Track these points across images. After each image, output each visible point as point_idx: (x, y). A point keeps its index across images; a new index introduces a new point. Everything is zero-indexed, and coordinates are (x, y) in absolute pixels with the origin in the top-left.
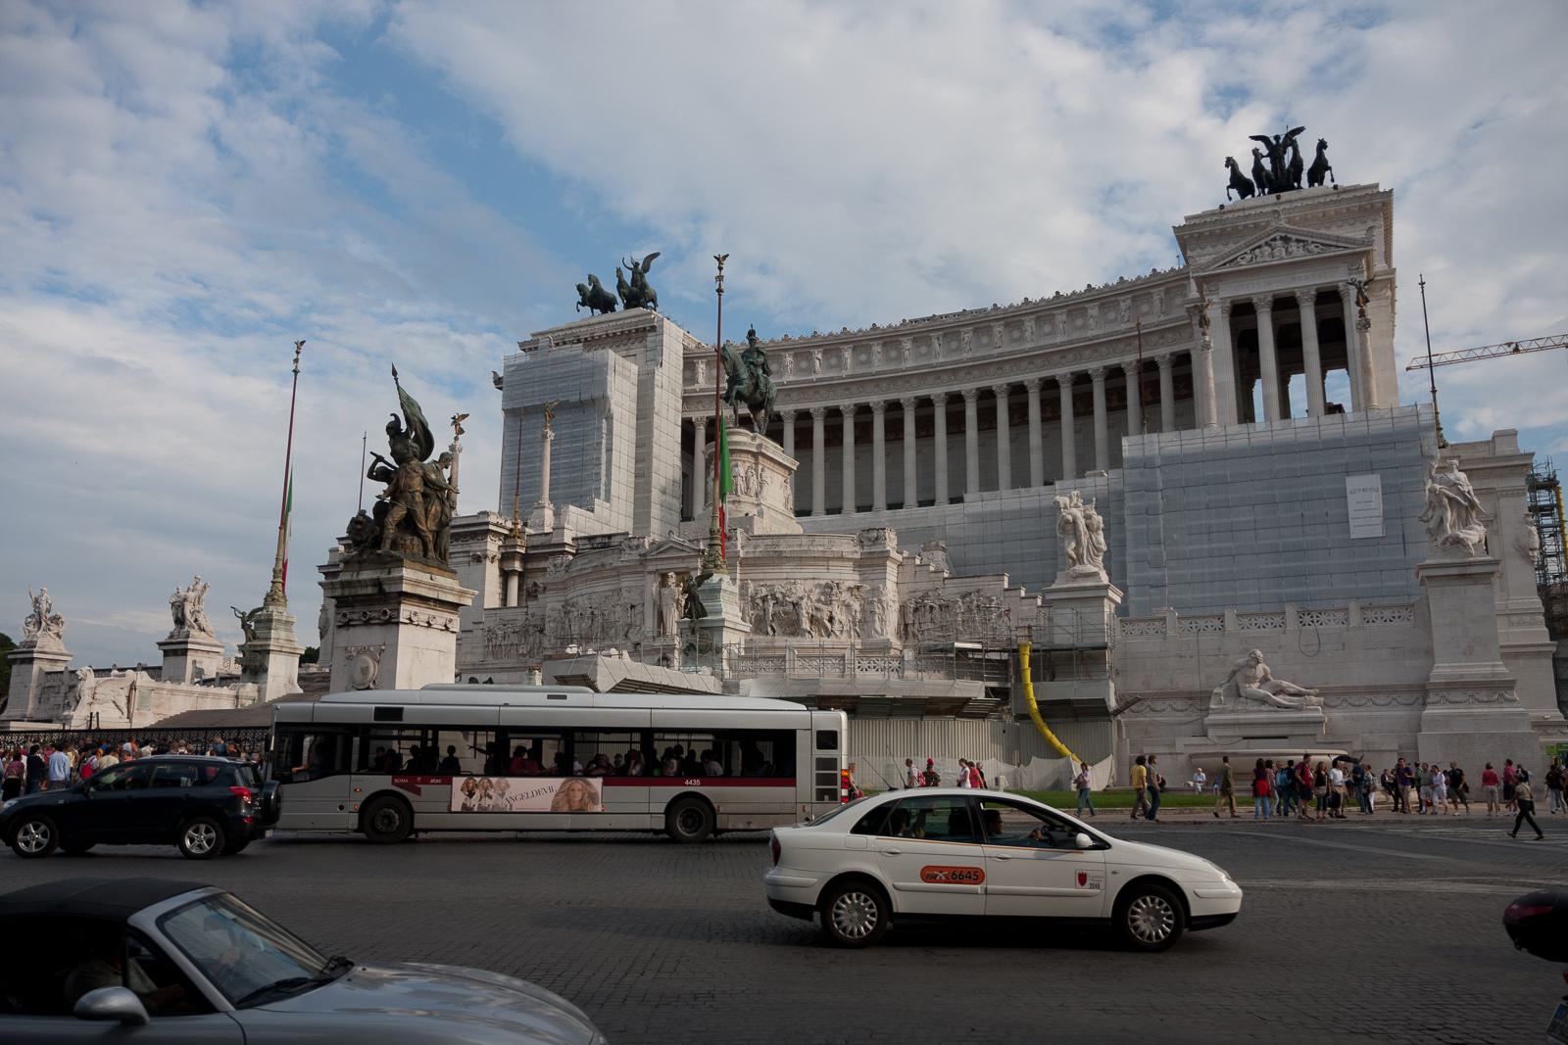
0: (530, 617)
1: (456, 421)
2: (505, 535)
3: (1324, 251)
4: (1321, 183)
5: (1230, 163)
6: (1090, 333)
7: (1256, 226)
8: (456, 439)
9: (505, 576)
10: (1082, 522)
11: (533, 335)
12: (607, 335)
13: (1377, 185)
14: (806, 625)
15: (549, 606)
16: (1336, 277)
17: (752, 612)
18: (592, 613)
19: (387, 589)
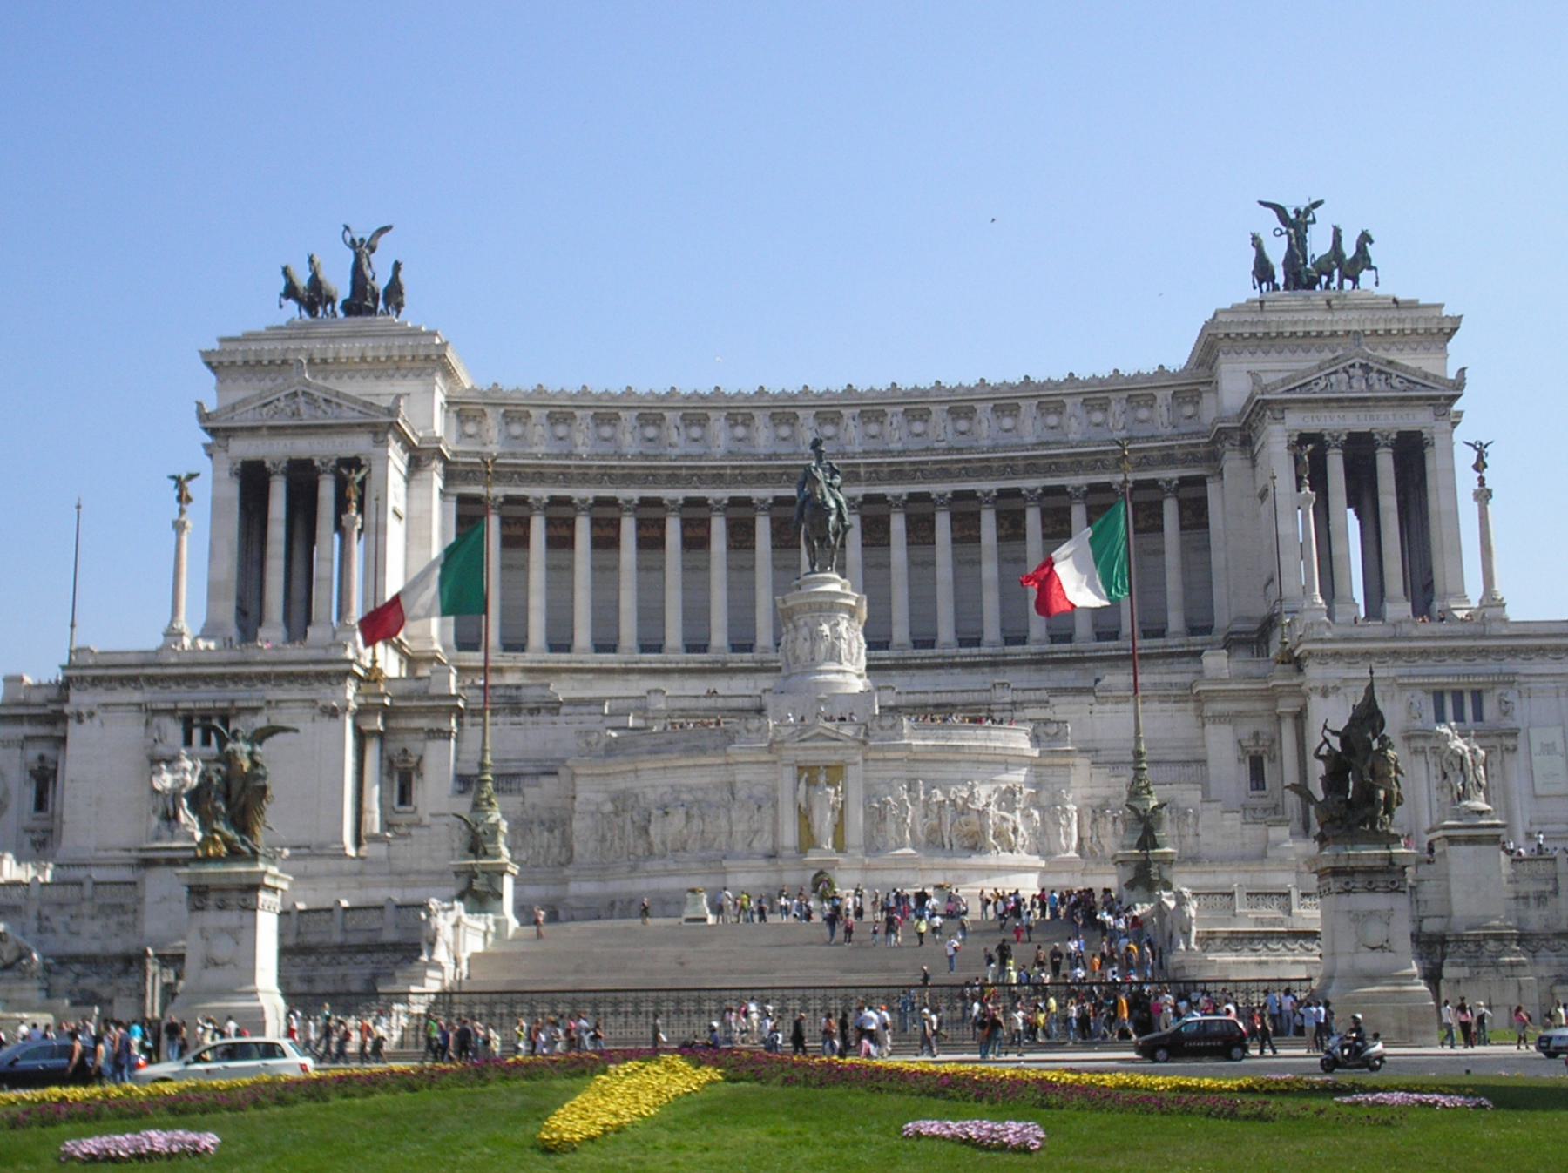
1: (180, 482)
2: (360, 678)
3: (1410, 389)
4: (1355, 281)
5: (1256, 242)
6: (1073, 437)
7: (1307, 334)
8: (182, 511)
9: (361, 737)
10: (1468, 756)
11: (222, 340)
12: (363, 359)
13: (1441, 306)
15: (580, 797)
16: (1417, 419)
19: (1397, 861)
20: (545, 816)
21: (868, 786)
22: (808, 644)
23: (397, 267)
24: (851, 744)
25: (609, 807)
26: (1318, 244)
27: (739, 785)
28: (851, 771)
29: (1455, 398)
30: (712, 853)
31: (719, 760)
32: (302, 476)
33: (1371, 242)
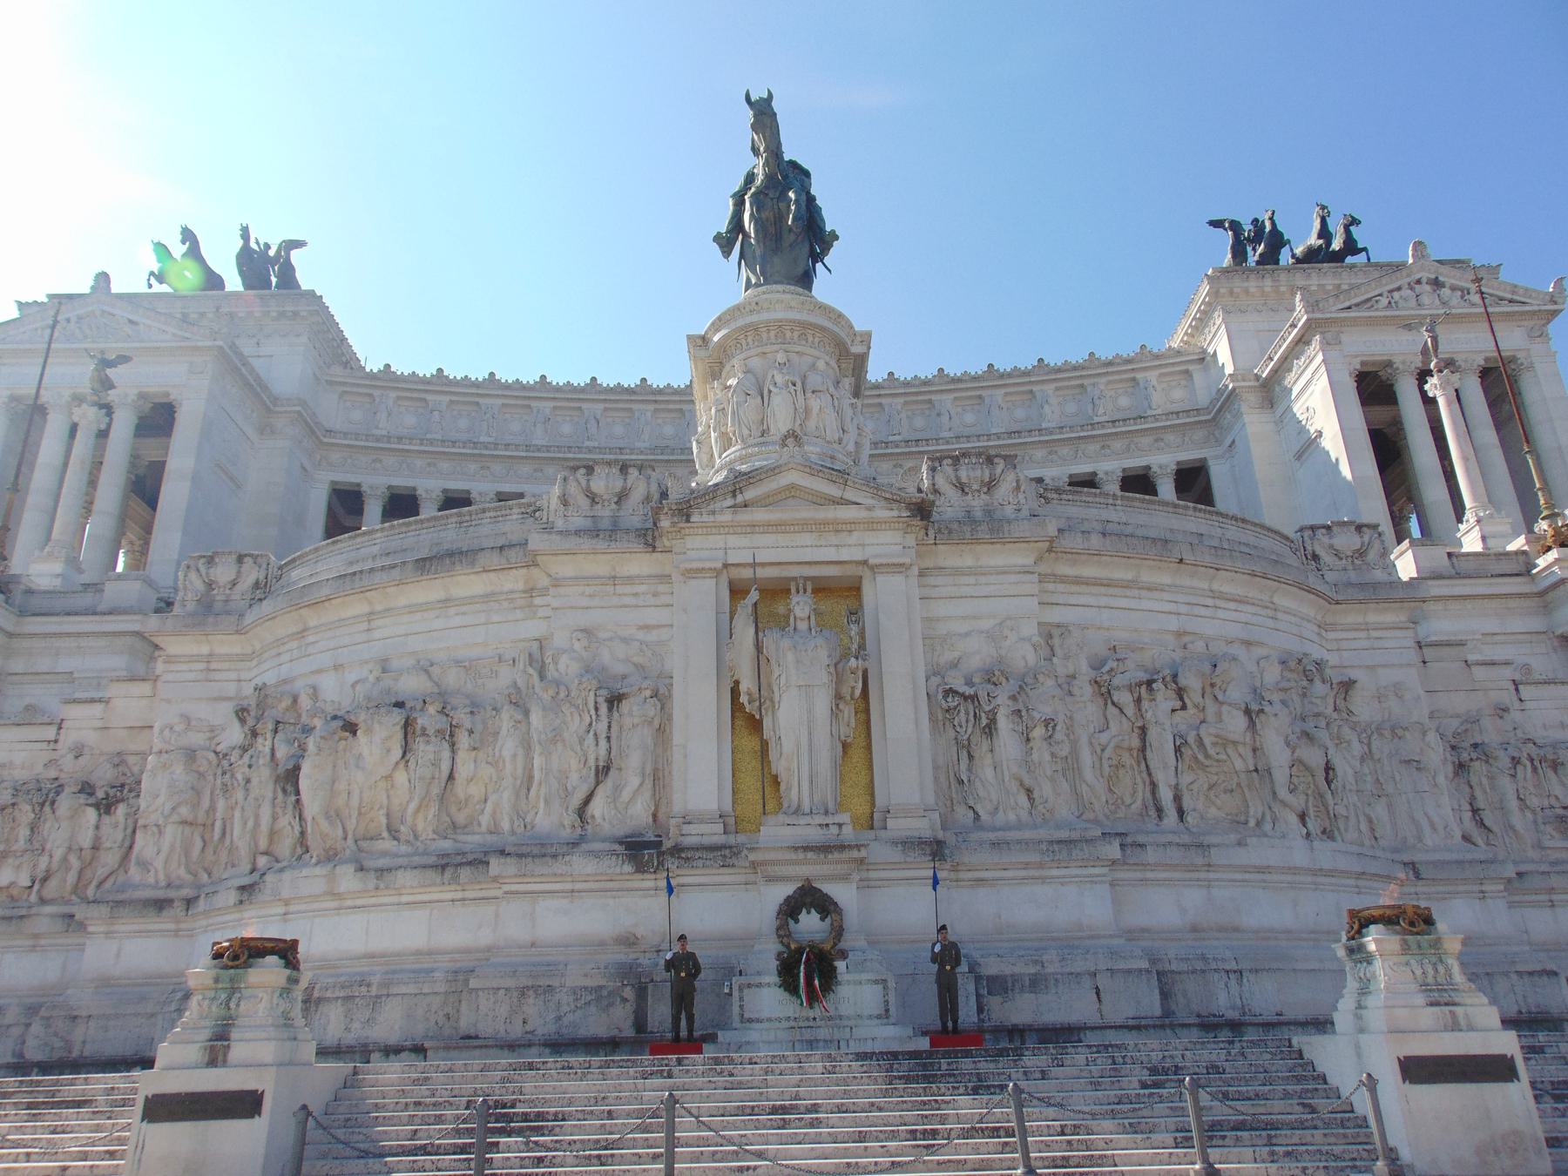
0: (68, 763)
14: (1283, 793)
17: (1104, 738)
18: (408, 725)
20: (104, 775)
21: (931, 641)
24: (882, 513)
27: (560, 640)
28: (886, 598)
30: (472, 840)
31: (513, 581)
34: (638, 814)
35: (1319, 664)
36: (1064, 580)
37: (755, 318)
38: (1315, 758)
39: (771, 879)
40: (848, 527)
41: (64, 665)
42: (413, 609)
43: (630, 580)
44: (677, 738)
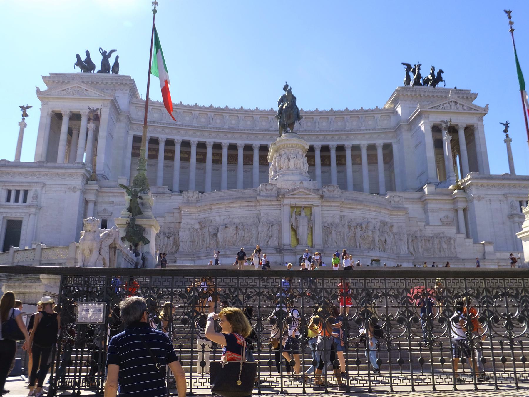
1: (24, 109)
2: (88, 180)
8: (23, 119)
11: (50, 74)
12: (102, 83)
14: (377, 244)
15: (183, 222)
18: (237, 227)
20: (166, 231)
21: (323, 218)
22: (287, 160)
23: (117, 57)
25: (197, 226)
26: (426, 74)
27: (262, 215)
28: (316, 211)
29: (485, 114)
32: (75, 117)
33: (443, 72)
34: (276, 243)
35: (387, 223)
36: (345, 208)
37: (287, 142)
38: (383, 239)
39: (298, 254)
40: (311, 198)
41: (111, 199)
42: (234, 207)
43: (273, 205)
44: (282, 232)
